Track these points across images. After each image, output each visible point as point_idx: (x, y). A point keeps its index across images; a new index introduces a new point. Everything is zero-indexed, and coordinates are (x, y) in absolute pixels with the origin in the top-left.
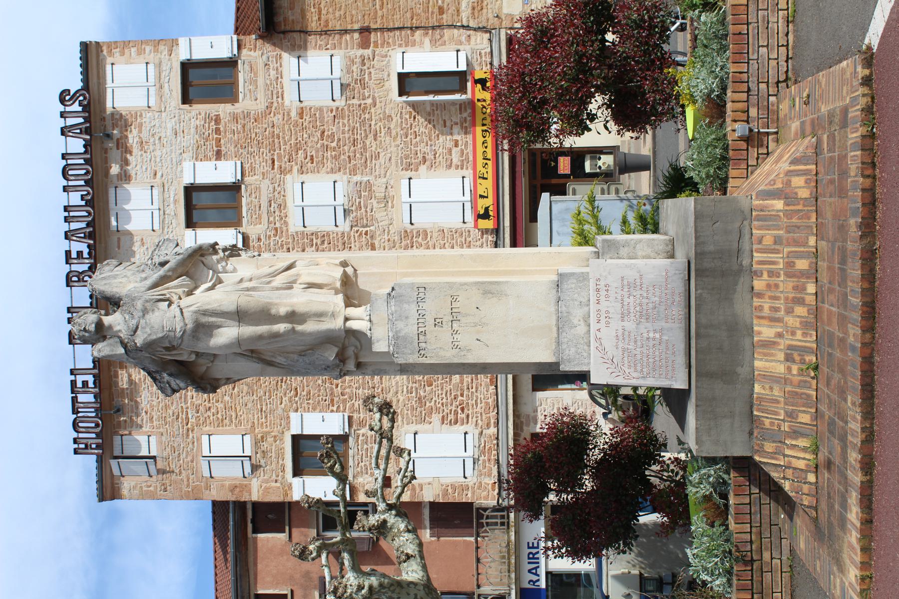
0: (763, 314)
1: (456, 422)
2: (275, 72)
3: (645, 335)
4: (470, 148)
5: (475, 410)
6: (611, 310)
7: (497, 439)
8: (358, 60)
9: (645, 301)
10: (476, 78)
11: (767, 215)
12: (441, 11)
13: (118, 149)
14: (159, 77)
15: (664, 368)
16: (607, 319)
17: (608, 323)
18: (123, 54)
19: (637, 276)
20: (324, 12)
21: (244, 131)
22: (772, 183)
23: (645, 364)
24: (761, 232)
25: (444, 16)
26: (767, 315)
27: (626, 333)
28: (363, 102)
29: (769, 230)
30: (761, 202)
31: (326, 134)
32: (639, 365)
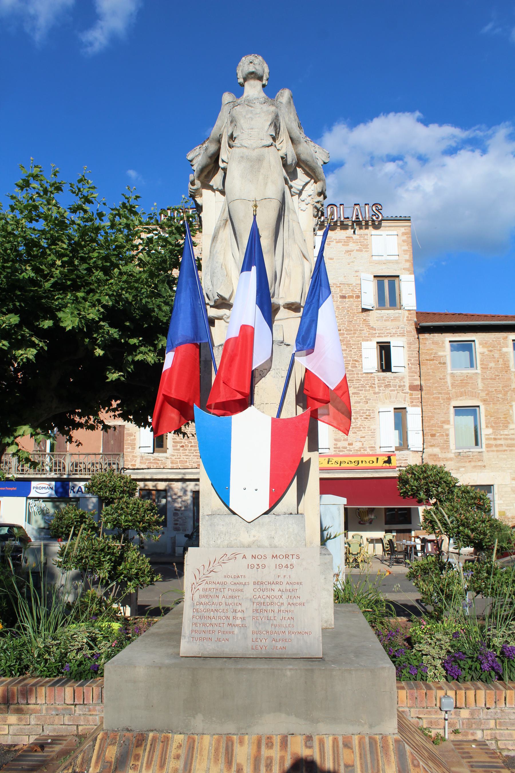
0: (263, 747)
1: (174, 442)
2: (394, 332)
3: (239, 608)
4: (346, 452)
5: (182, 454)
6: (266, 571)
7: (164, 468)
8: (402, 384)
9: (276, 608)
10: (391, 457)
11: (377, 755)
12: (433, 435)
13: (346, 237)
14: (389, 262)
15: (203, 628)
16: (256, 566)
17: (252, 567)
18: (404, 241)
19: (302, 600)
20: (431, 362)
21: (357, 313)
22: (416, 762)
23: (208, 607)
24: (357, 748)
25: (430, 437)
26: (262, 753)
27: (241, 587)
28: (376, 386)
29: (361, 758)
30: (391, 747)
31: (357, 363)
32: (207, 601)
